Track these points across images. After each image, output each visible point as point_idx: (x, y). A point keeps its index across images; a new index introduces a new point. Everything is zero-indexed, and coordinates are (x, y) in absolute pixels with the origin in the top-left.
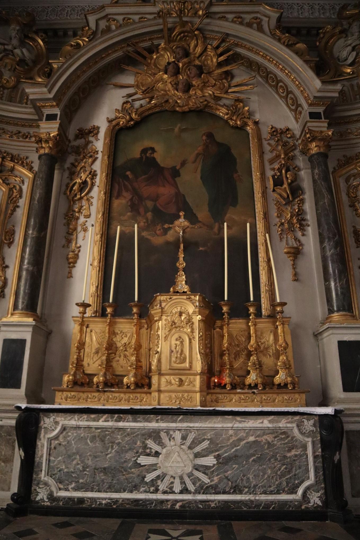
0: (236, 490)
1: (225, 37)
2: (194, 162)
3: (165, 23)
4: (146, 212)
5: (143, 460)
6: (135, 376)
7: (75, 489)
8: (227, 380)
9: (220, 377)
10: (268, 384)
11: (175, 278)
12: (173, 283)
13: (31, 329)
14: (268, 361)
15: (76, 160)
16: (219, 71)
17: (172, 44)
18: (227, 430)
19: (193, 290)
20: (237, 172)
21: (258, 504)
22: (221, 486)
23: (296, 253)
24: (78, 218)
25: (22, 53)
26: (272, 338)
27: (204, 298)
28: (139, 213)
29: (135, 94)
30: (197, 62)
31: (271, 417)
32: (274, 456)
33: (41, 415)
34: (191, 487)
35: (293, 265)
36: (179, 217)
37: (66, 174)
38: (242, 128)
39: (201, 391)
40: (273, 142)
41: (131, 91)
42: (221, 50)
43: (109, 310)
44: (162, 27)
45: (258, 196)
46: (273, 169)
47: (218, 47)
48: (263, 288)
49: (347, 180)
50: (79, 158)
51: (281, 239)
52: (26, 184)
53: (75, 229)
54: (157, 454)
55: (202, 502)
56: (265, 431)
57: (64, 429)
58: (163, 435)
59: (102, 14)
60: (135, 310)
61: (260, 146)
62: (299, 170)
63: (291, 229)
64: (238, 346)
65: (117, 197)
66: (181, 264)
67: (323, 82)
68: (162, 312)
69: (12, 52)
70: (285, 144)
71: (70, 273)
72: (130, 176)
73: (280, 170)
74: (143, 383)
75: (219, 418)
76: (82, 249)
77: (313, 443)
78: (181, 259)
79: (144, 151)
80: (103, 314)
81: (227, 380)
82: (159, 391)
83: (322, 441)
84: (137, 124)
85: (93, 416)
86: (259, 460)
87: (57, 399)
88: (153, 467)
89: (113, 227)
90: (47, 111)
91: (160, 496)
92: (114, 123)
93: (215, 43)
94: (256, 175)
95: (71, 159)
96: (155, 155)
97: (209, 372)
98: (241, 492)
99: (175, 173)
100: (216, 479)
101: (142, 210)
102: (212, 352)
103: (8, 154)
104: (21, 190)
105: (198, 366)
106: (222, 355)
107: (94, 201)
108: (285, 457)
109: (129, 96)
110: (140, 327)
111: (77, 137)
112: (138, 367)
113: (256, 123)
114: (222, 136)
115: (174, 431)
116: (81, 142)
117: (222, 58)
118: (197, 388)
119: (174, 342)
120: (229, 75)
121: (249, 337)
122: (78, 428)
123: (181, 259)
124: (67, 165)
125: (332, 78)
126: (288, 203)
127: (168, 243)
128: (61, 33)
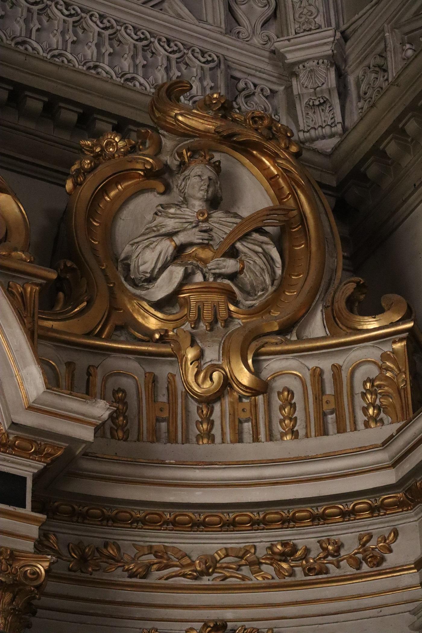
67: (53, 381)
125: (89, 335)
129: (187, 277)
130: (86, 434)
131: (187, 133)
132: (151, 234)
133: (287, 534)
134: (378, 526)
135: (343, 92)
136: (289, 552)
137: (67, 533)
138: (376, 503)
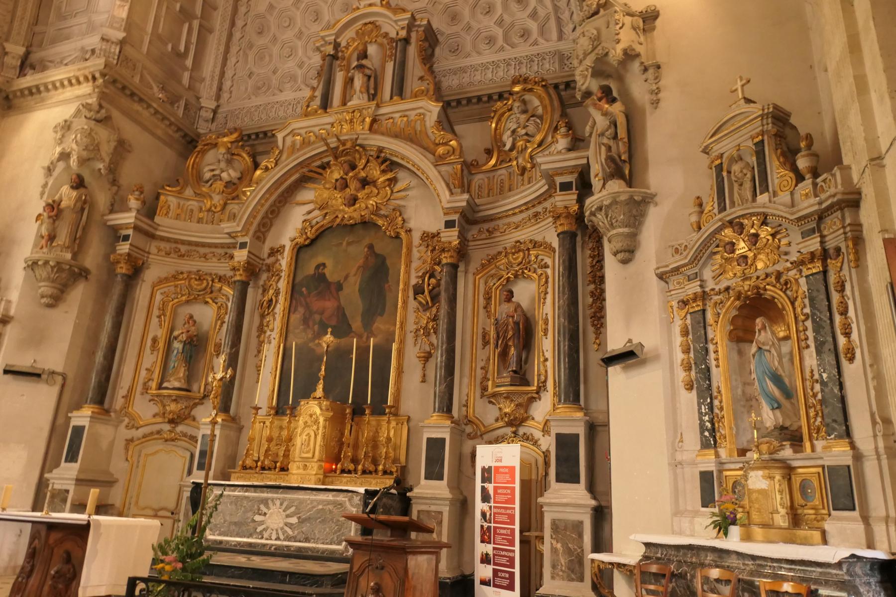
0: (307, 540)
1: (380, 150)
2: (355, 275)
3: (327, 144)
4: (314, 325)
5: (258, 518)
7: (219, 535)
11: (316, 386)
12: (315, 390)
17: (339, 160)
18: (304, 501)
20: (388, 282)
21: (318, 550)
22: (298, 537)
24: (265, 332)
25: (229, 175)
28: (308, 326)
29: (314, 210)
30: (363, 174)
32: (332, 519)
34: (282, 537)
37: (260, 291)
38: (397, 237)
40: (423, 248)
42: (380, 160)
44: (325, 148)
46: (418, 277)
47: (378, 157)
51: (415, 345)
54: (265, 514)
55: (287, 546)
56: (329, 503)
58: (270, 502)
65: (294, 313)
66: (323, 372)
73: (422, 277)
75: (303, 492)
78: (323, 368)
79: (318, 267)
84: (313, 241)
86: (323, 521)
88: (262, 523)
89: (289, 339)
91: (263, 541)
92: (294, 243)
94: (401, 286)
95: (264, 276)
98: (309, 542)
99: (339, 287)
100: (296, 532)
101: (311, 323)
108: (338, 521)
109: (309, 213)
113: (409, 231)
115: (276, 499)
116: (272, 259)
117: (383, 167)
119: (304, 437)
120: (393, 181)
124: (261, 283)
129: (514, 140)
131: (517, 93)
133: (535, 210)
137: (486, 226)
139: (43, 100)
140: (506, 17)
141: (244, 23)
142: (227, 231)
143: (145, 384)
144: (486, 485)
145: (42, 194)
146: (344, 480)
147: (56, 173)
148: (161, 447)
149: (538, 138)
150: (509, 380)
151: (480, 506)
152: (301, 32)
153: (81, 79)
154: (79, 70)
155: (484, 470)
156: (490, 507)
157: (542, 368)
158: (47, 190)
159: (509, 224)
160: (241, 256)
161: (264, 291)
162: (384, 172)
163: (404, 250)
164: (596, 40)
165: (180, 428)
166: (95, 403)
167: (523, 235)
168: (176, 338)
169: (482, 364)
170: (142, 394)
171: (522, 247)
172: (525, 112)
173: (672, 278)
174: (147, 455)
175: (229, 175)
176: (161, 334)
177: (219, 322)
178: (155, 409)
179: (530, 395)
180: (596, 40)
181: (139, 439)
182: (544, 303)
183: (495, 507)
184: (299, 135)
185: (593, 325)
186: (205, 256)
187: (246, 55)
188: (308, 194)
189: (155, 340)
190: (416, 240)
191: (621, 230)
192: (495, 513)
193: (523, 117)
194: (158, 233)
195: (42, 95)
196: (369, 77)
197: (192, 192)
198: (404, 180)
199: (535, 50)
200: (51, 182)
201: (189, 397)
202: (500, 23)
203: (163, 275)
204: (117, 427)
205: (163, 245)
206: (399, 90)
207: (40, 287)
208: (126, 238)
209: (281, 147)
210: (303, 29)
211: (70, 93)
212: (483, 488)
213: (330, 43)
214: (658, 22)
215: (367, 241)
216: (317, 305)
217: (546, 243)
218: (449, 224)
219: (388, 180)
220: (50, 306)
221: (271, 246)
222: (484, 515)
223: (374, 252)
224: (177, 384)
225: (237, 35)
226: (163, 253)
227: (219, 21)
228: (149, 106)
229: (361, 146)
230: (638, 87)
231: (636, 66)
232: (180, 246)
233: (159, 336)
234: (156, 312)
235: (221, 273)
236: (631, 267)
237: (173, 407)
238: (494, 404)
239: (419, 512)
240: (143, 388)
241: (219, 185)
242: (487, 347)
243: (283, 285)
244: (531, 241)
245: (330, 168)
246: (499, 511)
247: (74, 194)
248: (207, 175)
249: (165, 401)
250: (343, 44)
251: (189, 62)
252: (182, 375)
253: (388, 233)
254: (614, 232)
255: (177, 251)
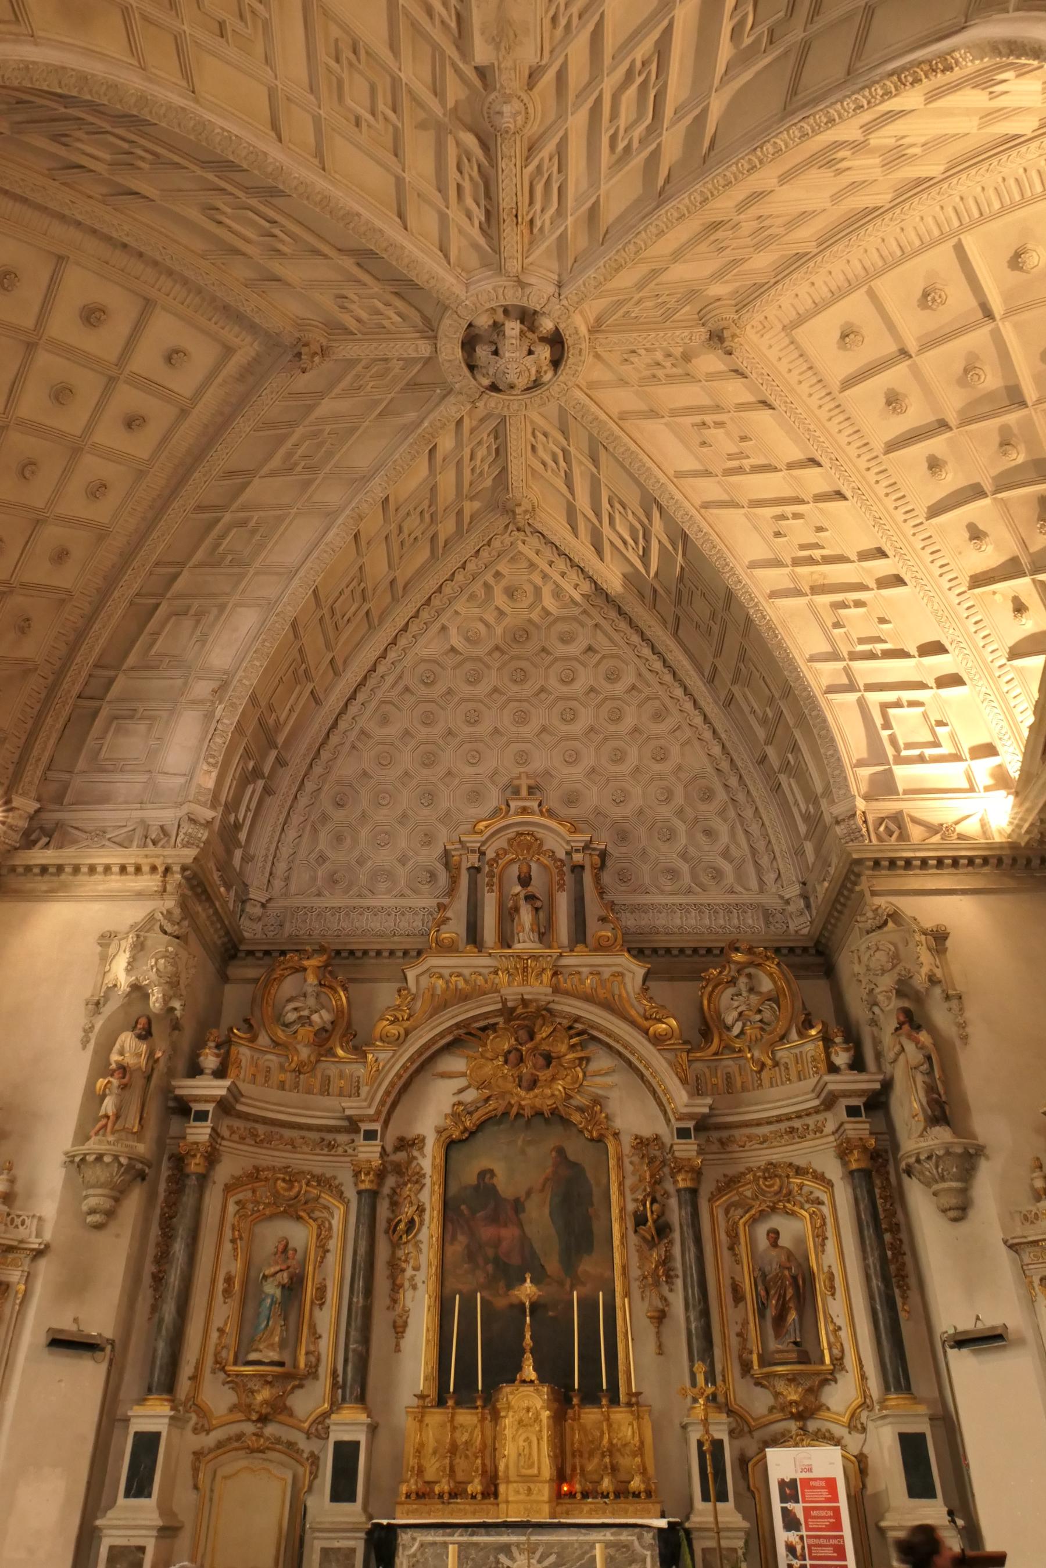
1: (578, 1019)
2: (542, 1190)
6: (481, 1483)
8: (578, 1487)
9: (571, 1484)
10: (622, 1493)
12: (519, 1368)
13: (365, 1428)
14: (626, 1462)
15: (399, 1186)
16: (570, 1056)
18: (571, 1543)
19: (542, 1380)
20: (592, 1205)
23: (660, 1317)
24: (403, 1271)
26: (630, 1433)
27: (552, 1389)
30: (545, 1047)
31: (614, 1530)
33: (399, 1531)
35: (658, 1333)
36: (525, 1281)
38: (600, 1140)
39: (550, 1501)
40: (636, 1159)
41: (462, 1082)
43: (450, 1403)
44: (499, 1006)
45: (616, 1242)
46: (636, 1200)
47: (570, 1028)
48: (621, 1367)
49: (727, 1212)
50: (401, 1181)
52: (336, 1217)
53: (401, 1286)
57: (422, 1545)
58: (514, 1549)
59: (424, 967)
60: (479, 1403)
61: (620, 1166)
62: (669, 1197)
63: (657, 1284)
64: (592, 1442)
67: (691, 1095)
68: (509, 1407)
69: (308, 1018)
70: (652, 1161)
71: (397, 1345)
72: (466, 1212)
74: (491, 1492)
75: (565, 1530)
76: (411, 1314)
77: (652, 1557)
78: (528, 1335)
79: (482, 1174)
80: (441, 1402)
81: (578, 1487)
82: (507, 1502)
83: (661, 1555)
85: (448, 1531)
87: (398, 1514)
90: (364, 1126)
92: (445, 1135)
93: (566, 1023)
95: (391, 1181)
96: (495, 1181)
97: (561, 1476)
99: (518, 1206)
102: (563, 1452)
103: (313, 1176)
104: (330, 1228)
105: (547, 1470)
106: (574, 1456)
107: (424, 1247)
109: (461, 1091)
110: (482, 1420)
111: (398, 1149)
112: (484, 1473)
114: (576, 1149)
116: (401, 1156)
117: (573, 1041)
118: (546, 1498)
121: (602, 1433)
122: (434, 1544)
123: (528, 1335)
126: (652, 1244)
127: (512, 1306)
128: (359, 954)
129: (744, 1025)
130: (706, 1110)
131: (738, 963)
132: (731, 1005)
134: (820, 1117)
135: (808, 906)
136: (792, 1131)
137: (715, 1135)
138: (817, 1111)
139: (64, 887)
140: (692, 850)
141: (316, 787)
142: (348, 1112)
143: (216, 1354)
144: (790, 1506)
145: (85, 1043)
146: (586, 1508)
147: (108, 1010)
148: (243, 1463)
149: (780, 1028)
150: (794, 1355)
151: (782, 1537)
152: (404, 815)
153: (146, 869)
154: (146, 856)
155: (782, 1484)
156: (801, 1538)
157: (832, 1339)
158: (93, 1036)
159: (750, 1138)
160: (369, 1152)
161: (394, 1205)
162: (572, 1047)
163: (612, 1163)
164: (895, 958)
165: (270, 1430)
166: (160, 1391)
167: (781, 1153)
168: (265, 1277)
169: (738, 1328)
170: (213, 1372)
171: (780, 1172)
172: (751, 990)
173: (1028, 1250)
174: (225, 1478)
175: (321, 1017)
176: (236, 1267)
177: (321, 1253)
178: (230, 1397)
179: (822, 1377)
180: (895, 958)
181: (211, 1451)
182: (823, 1251)
183: (808, 1537)
184: (441, 976)
185: (899, 1287)
186: (292, 1143)
187: (315, 830)
188: (456, 1063)
189: (229, 1280)
190: (627, 1149)
191: (954, 1184)
192: (809, 1546)
193: (754, 999)
194: (239, 1107)
195: (63, 877)
196: (537, 909)
197: (267, 1038)
198: (602, 1062)
199: (732, 898)
200: (99, 1023)
201: (290, 1377)
202: (684, 856)
203: (238, 1173)
204: (183, 1429)
205: (237, 1123)
206: (579, 934)
207: (86, 1197)
208: (202, 1116)
209: (414, 990)
210: (410, 812)
211: (115, 882)
212: (785, 1512)
213: (473, 851)
214: (949, 943)
215: (552, 1143)
216: (487, 1233)
217: (815, 1171)
218: (683, 1134)
219: (581, 1059)
220: (99, 1227)
221: (398, 1134)
222: (791, 1549)
223: (566, 1158)
224: (274, 1356)
225: (303, 801)
226: (236, 1137)
227: (286, 782)
228: (213, 905)
229: (549, 1011)
230: (940, 1016)
231: (937, 991)
232: (257, 1126)
233: (233, 1273)
234: (228, 1234)
235: (317, 1171)
236: (963, 1227)
237: (264, 1394)
238: (763, 1386)
239: (703, 1550)
240: (216, 1362)
241: (305, 1033)
242: (741, 1305)
243: (430, 1197)
244: (791, 1164)
245: (495, 1031)
246: (817, 1541)
247: (144, 1047)
248: (291, 1017)
249: (250, 1385)
250: (490, 854)
251: (243, 836)
252: (277, 1339)
253: (587, 1134)
254: (946, 1185)
255: (254, 1135)
